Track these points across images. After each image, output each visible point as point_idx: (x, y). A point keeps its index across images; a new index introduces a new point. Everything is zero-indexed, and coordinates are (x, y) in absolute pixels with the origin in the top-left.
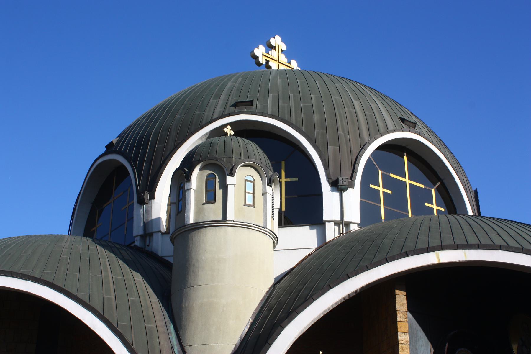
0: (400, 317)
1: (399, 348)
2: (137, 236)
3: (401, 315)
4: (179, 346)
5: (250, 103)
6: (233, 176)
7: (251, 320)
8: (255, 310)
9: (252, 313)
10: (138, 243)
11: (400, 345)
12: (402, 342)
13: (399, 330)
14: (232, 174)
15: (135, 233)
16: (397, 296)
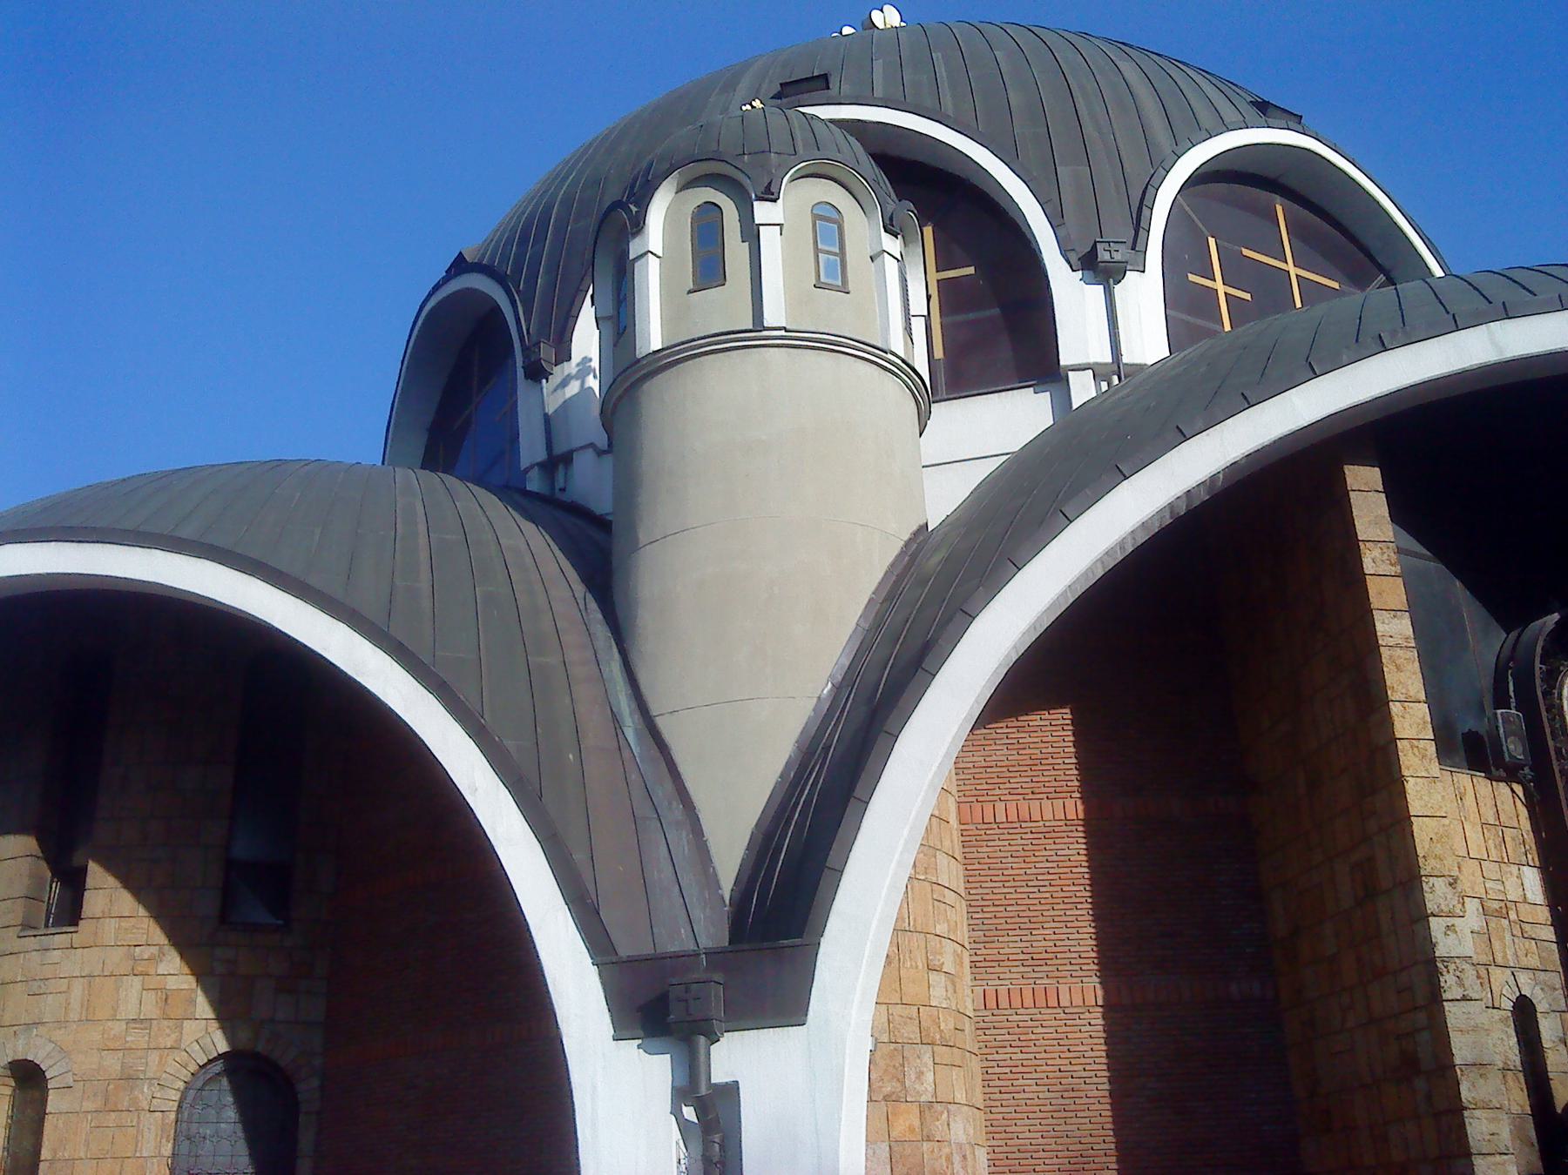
0: (1374, 562)
1: (1384, 661)
2: (532, 467)
3: (1376, 553)
4: (637, 716)
5: (821, 83)
6: (775, 201)
7: (863, 624)
8: (873, 593)
9: (866, 602)
10: (534, 483)
11: (1385, 652)
12: (1391, 642)
13: (1375, 602)
14: (770, 195)
15: (525, 462)
16: (1352, 494)
